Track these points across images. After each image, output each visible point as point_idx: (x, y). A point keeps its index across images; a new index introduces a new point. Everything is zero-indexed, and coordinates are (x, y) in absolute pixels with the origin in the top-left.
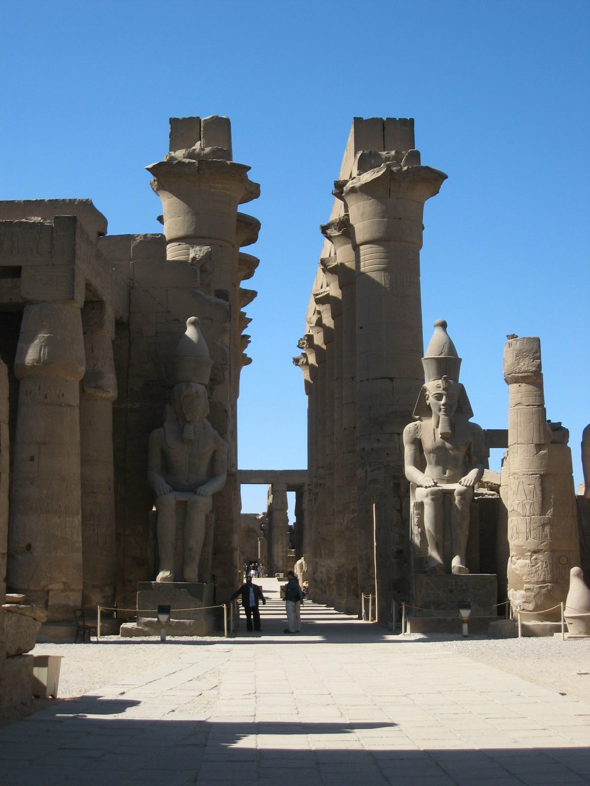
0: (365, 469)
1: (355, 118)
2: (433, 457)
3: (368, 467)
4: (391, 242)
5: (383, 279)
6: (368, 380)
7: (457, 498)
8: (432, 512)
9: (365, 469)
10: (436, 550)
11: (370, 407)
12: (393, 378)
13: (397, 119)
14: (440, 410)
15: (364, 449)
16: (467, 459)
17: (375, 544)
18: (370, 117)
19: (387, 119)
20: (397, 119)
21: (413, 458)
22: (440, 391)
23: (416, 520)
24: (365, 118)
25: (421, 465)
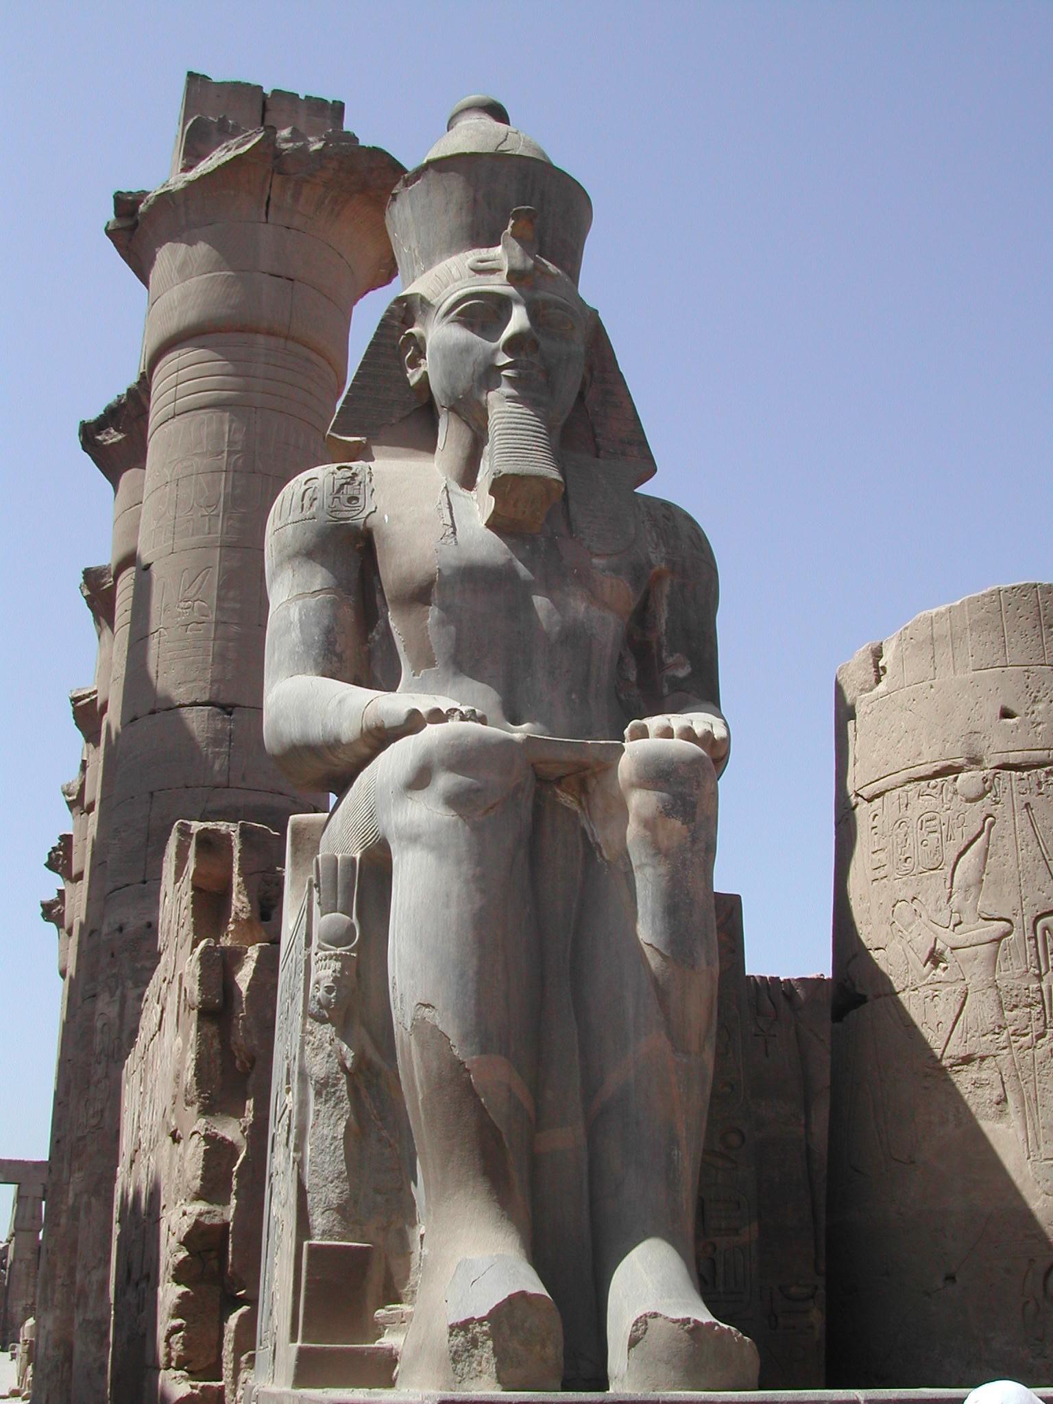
0: (118, 993)
1: (191, 75)
2: (442, 623)
3: (130, 984)
4: (259, 336)
5: (227, 428)
6: (153, 712)
7: (640, 802)
8: (456, 887)
9: (118, 993)
10: (483, 1186)
11: (152, 793)
12: (234, 706)
13: (302, 97)
14: (489, 376)
15: (121, 929)
16: (632, 675)
17: (116, 1229)
18: (234, 80)
19: (274, 91)
20: (302, 97)
21: (316, 634)
22: (498, 284)
23: (325, 973)
24: (216, 78)
25: (358, 652)
